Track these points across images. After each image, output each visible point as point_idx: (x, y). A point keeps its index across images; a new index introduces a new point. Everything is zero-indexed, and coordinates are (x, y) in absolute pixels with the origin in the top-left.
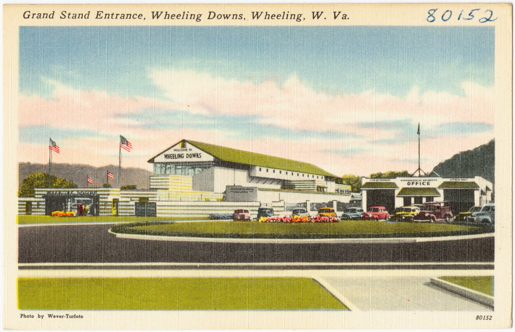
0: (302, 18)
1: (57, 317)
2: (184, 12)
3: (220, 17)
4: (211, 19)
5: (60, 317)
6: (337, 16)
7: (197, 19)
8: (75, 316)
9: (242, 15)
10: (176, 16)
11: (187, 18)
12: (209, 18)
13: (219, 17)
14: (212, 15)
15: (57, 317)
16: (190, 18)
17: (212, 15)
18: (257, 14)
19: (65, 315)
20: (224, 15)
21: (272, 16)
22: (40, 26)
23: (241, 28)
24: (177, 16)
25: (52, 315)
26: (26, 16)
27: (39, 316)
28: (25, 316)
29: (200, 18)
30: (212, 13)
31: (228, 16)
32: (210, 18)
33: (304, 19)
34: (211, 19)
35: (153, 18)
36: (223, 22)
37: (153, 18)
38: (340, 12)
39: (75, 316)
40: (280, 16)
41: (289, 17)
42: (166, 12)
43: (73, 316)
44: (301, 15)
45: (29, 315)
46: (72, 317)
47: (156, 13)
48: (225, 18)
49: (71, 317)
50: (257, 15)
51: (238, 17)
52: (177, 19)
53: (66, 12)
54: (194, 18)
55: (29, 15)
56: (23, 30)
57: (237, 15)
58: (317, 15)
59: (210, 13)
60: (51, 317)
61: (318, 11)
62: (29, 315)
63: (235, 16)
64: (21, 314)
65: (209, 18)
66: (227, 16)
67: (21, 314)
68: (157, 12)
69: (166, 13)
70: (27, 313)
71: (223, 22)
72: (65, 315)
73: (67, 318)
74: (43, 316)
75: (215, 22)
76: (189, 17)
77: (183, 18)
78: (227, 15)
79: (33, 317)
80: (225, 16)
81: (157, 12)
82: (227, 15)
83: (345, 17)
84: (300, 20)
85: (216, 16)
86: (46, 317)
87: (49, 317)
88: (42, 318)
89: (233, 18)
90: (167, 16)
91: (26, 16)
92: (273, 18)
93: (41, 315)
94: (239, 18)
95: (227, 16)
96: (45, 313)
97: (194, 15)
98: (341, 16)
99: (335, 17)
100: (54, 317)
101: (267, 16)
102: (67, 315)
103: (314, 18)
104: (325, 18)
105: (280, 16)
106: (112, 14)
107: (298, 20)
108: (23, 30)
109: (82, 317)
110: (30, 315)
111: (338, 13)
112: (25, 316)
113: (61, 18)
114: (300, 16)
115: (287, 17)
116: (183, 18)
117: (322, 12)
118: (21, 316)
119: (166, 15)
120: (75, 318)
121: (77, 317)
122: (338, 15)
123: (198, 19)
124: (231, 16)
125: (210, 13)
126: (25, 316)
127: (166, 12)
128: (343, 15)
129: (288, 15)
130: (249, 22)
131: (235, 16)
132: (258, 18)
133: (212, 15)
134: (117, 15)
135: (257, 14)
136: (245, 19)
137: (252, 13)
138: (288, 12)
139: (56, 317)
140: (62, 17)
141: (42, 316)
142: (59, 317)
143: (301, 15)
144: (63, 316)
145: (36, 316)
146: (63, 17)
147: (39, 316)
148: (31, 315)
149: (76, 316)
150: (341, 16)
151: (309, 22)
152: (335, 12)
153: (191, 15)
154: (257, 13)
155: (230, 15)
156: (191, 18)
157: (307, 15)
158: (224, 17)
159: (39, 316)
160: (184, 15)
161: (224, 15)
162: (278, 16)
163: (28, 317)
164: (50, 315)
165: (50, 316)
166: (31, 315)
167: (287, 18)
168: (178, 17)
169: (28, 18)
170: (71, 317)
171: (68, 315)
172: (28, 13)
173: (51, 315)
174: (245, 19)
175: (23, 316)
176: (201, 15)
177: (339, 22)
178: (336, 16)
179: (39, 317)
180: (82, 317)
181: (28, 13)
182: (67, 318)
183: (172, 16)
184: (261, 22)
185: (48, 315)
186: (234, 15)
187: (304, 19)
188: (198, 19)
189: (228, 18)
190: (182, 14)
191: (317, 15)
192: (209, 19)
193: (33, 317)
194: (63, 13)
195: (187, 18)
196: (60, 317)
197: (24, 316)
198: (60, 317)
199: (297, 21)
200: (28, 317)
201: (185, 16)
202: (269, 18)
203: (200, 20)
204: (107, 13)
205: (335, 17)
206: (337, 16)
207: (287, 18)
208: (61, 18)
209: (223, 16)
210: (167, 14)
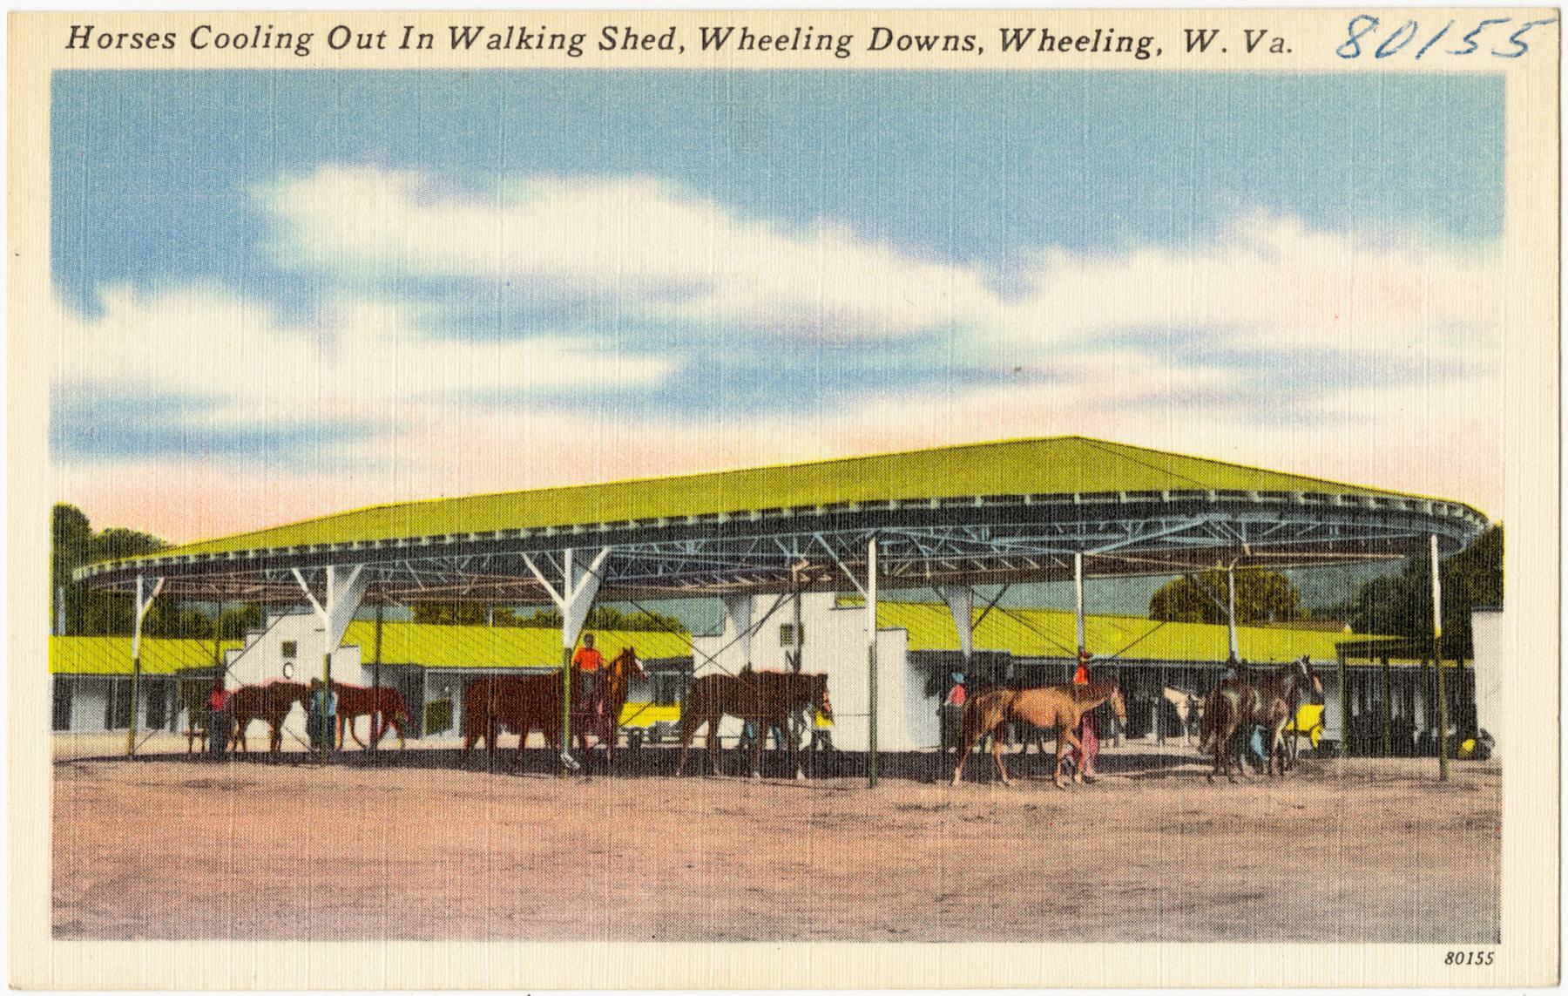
0: (1151, 49)
2: (798, 30)
3: (904, 43)
4: (879, 49)
6: (474, 39)
7: (572, 48)
9: (974, 37)
10: (774, 41)
12: (872, 48)
13: (905, 43)
14: (883, 37)
16: (549, 44)
17: (883, 36)
20: (918, 38)
21: (1062, 42)
23: (971, 77)
24: (778, 42)
29: (847, 47)
30: (881, 31)
32: (876, 46)
33: (1160, 51)
34: (879, 49)
36: (915, 59)
38: (480, 28)
40: (787, 40)
44: (1149, 40)
48: (920, 47)
50: (470, 39)
51: (962, 43)
52: (644, 51)
56: (64, 84)
57: (957, 38)
58: (1198, 40)
59: (877, 30)
63: (952, 42)
65: (872, 48)
66: (927, 42)
68: (717, 30)
71: (915, 59)
75: (892, 59)
77: (794, 48)
78: (927, 38)
80: (922, 41)
81: (717, 30)
82: (927, 38)
83: (1279, 46)
84: (1148, 55)
85: (895, 41)
89: (945, 48)
90: (631, 40)
94: (964, 49)
95: (927, 42)
97: (563, 37)
98: (1267, 42)
99: (1250, 48)
101: (747, 42)
107: (573, 52)
108: (64, 84)
114: (1148, 44)
115: (267, 41)
116: (794, 48)
117: (1215, 32)
123: (843, 50)
124: (941, 42)
125: (877, 30)
128: (492, 37)
130: (995, 59)
131: (952, 42)
133: (883, 36)
136: (981, 50)
143: (1149, 40)
150: (484, 38)
151: (1173, 57)
152: (1248, 32)
153: (821, 37)
155: (936, 38)
156: (819, 48)
157: (990, 39)
158: (919, 45)
160: (796, 39)
161: (918, 38)
167: (1107, 49)
168: (781, 46)
174: (981, 50)
176: (849, 38)
177: (1262, 59)
183: (761, 42)
184: (1030, 58)
186: (948, 38)
187: (1160, 51)
190: (792, 36)
192: (876, 52)
195: (807, 47)
199: (569, 53)
202: (751, 47)
203: (581, 52)
204: (285, 33)
205: (1250, 48)
206: (474, 39)
209: (914, 41)
210: (632, 33)
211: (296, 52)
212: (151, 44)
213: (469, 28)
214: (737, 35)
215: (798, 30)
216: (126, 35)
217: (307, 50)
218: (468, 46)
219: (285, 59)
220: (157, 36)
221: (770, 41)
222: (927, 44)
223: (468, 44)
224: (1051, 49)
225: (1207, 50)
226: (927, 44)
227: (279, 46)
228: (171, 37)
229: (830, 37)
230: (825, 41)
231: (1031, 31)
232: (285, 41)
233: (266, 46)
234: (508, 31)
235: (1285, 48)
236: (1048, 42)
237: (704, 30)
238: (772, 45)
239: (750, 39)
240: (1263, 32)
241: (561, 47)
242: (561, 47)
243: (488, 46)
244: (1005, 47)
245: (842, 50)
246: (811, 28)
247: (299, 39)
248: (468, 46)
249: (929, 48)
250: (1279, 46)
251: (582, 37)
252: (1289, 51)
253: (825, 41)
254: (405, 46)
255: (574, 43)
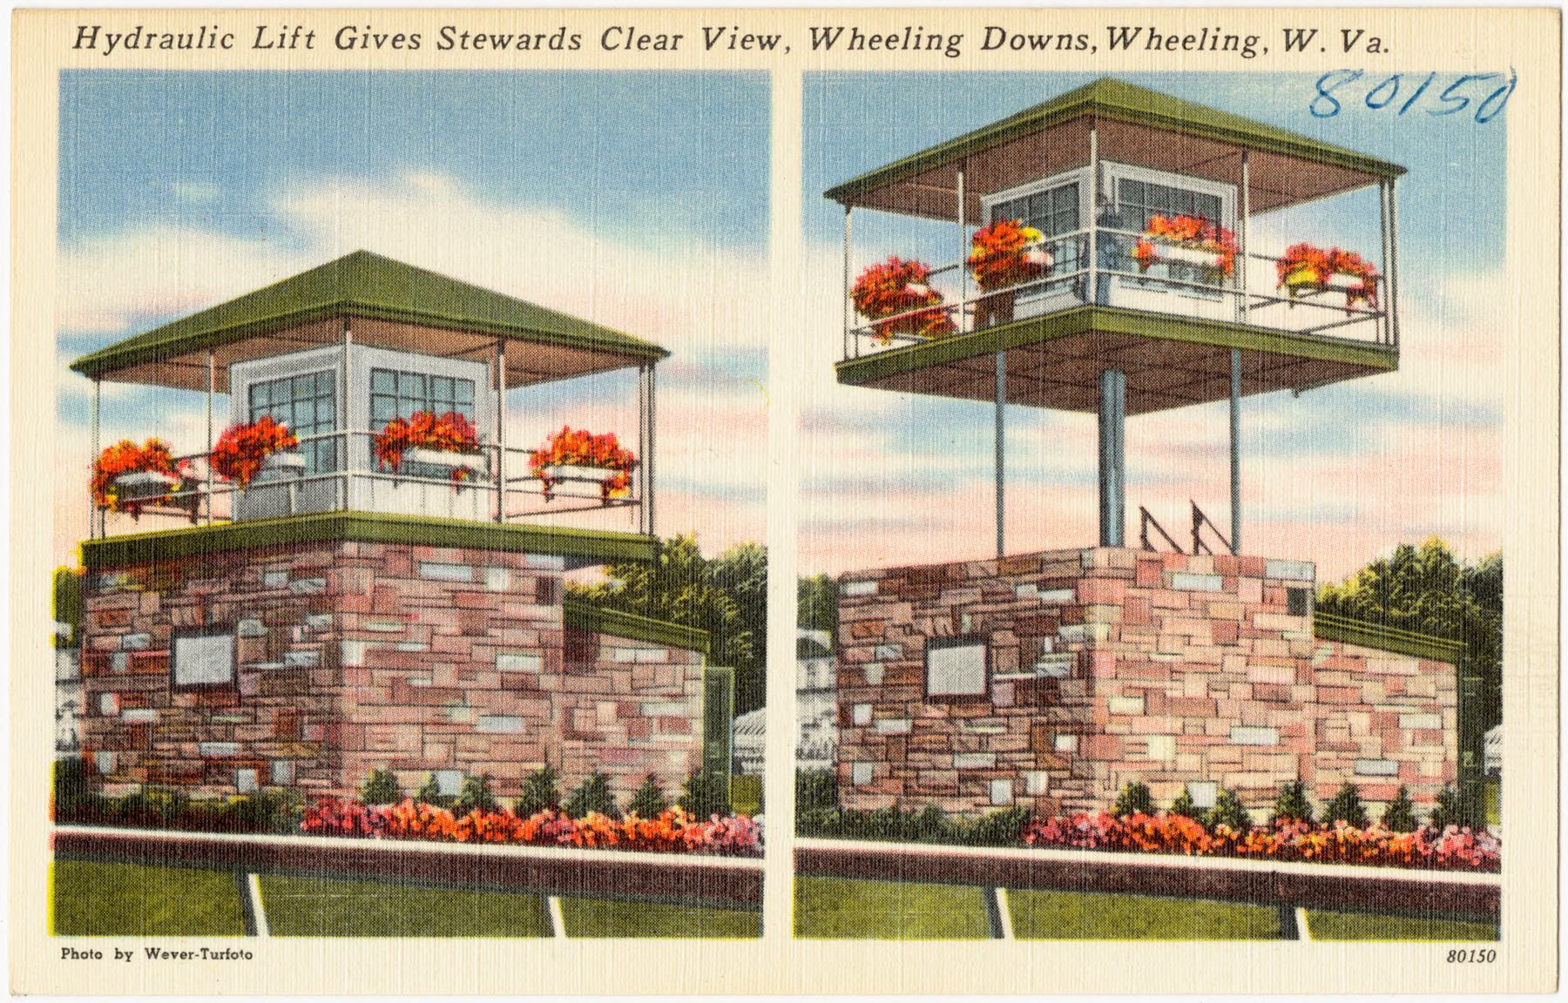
0: (1258, 48)
1: (174, 957)
2: (909, 29)
5: (183, 956)
8: (229, 955)
10: (884, 40)
11: (917, 47)
12: (986, 47)
13: (1017, 43)
15: (174, 957)
18: (1124, 34)
19: (198, 951)
20: (1031, 37)
22: (286, 69)
24: (888, 40)
25: (159, 949)
26: (344, 41)
27: (118, 955)
28: (77, 953)
31: (1044, 40)
32: (990, 45)
33: (1266, 50)
35: (815, 48)
37: (815, 48)
39: (229, 955)
41: (1221, 42)
42: (855, 30)
43: (222, 953)
44: (1255, 39)
45: (89, 952)
46: (219, 956)
47: (823, 32)
48: (1033, 46)
49: (215, 957)
53: (453, 29)
54: (938, 48)
55: (353, 40)
58: (1297, 40)
59: (989, 29)
60: (156, 957)
61: (828, 26)
62: (89, 952)
64: (64, 949)
65: (986, 47)
66: (1040, 41)
67: (64, 949)
69: (855, 33)
70: (81, 943)
72: (198, 951)
73: (205, 958)
74: (131, 953)
76: (924, 43)
77: (905, 47)
79: (99, 956)
80: (1035, 40)
82: (1040, 37)
86: (140, 955)
87: (149, 957)
88: (128, 961)
91: (344, 41)
92: (479, 44)
93: (122, 951)
95: (1040, 41)
96: (136, 944)
100: (165, 955)
102: (204, 950)
103: (1288, 47)
104: (1323, 50)
105: (1194, 40)
106: (465, 36)
109: (249, 956)
110: (91, 953)
111: (1134, 31)
112: (75, 955)
113: (440, 47)
116: (905, 47)
118: (64, 954)
119: (855, 37)
120: (228, 958)
121: (234, 956)
122: (1310, 37)
123: (953, 50)
126: (75, 955)
127: (855, 30)
129: (1215, 38)
132: (1126, 45)
133: (995, 37)
134: (539, 37)
135: (1124, 34)
137: (1109, 31)
138: (921, 28)
139: (171, 956)
140: (442, 44)
141: (129, 955)
142: (178, 956)
144: (190, 954)
145: (109, 954)
146: (446, 44)
147: (117, 953)
148: (94, 952)
149: (231, 951)
151: (1276, 59)
153: (931, 37)
154: (1125, 30)
155: (1049, 37)
159: (118, 955)
160: (910, 39)
161: (1031, 37)
162: (1185, 41)
163: (85, 955)
164: (153, 949)
165: (152, 953)
166: (94, 952)
168: (892, 45)
169: (351, 46)
170: (216, 958)
171: (207, 949)
172: (348, 34)
173: (156, 951)
175: (70, 954)
176: (959, 37)
178: (711, 40)
179: (116, 957)
180: (249, 956)
181: (348, 34)
182: (205, 958)
185: (147, 949)
186: (1061, 37)
187: (1266, 50)
188: (953, 50)
189: (1043, 47)
191: (1297, 40)
193: (99, 956)
194: (446, 31)
196: (183, 956)
197: (73, 953)
198: (181, 956)
200: (85, 955)
201: (912, 42)
207: (1213, 48)
208: (440, 47)
209: (1028, 41)
211: (1242, 54)
212: (1188, 45)
213: (830, 28)
214: (847, 36)
215: (909, 29)
216: (544, 36)
217: (1254, 53)
218: (1301, 49)
219: (935, 61)
220: (648, 37)
221: (880, 40)
222: (1040, 43)
223: (829, 45)
224: (1158, 47)
225: (1305, 50)
226: (1040, 43)
227: (1226, 48)
228: (416, 38)
229: (1237, 38)
230: (935, 42)
231: (1138, 29)
232: (935, 42)
233: (1213, 48)
234: (906, 31)
235: (1381, 49)
236: (1155, 41)
237: (1287, 31)
238: (883, 44)
239: (860, 39)
240: (1360, 32)
241: (1235, 48)
242: (1235, 48)
243: (1368, 49)
244: (1288, 47)
245: (952, 50)
246: (921, 28)
247: (1246, 41)
248: (1301, 49)
249: (1043, 47)
250: (1375, 46)
251: (959, 37)
252: (1386, 51)
253: (1232, 42)
254: (732, 47)
255: (951, 44)
